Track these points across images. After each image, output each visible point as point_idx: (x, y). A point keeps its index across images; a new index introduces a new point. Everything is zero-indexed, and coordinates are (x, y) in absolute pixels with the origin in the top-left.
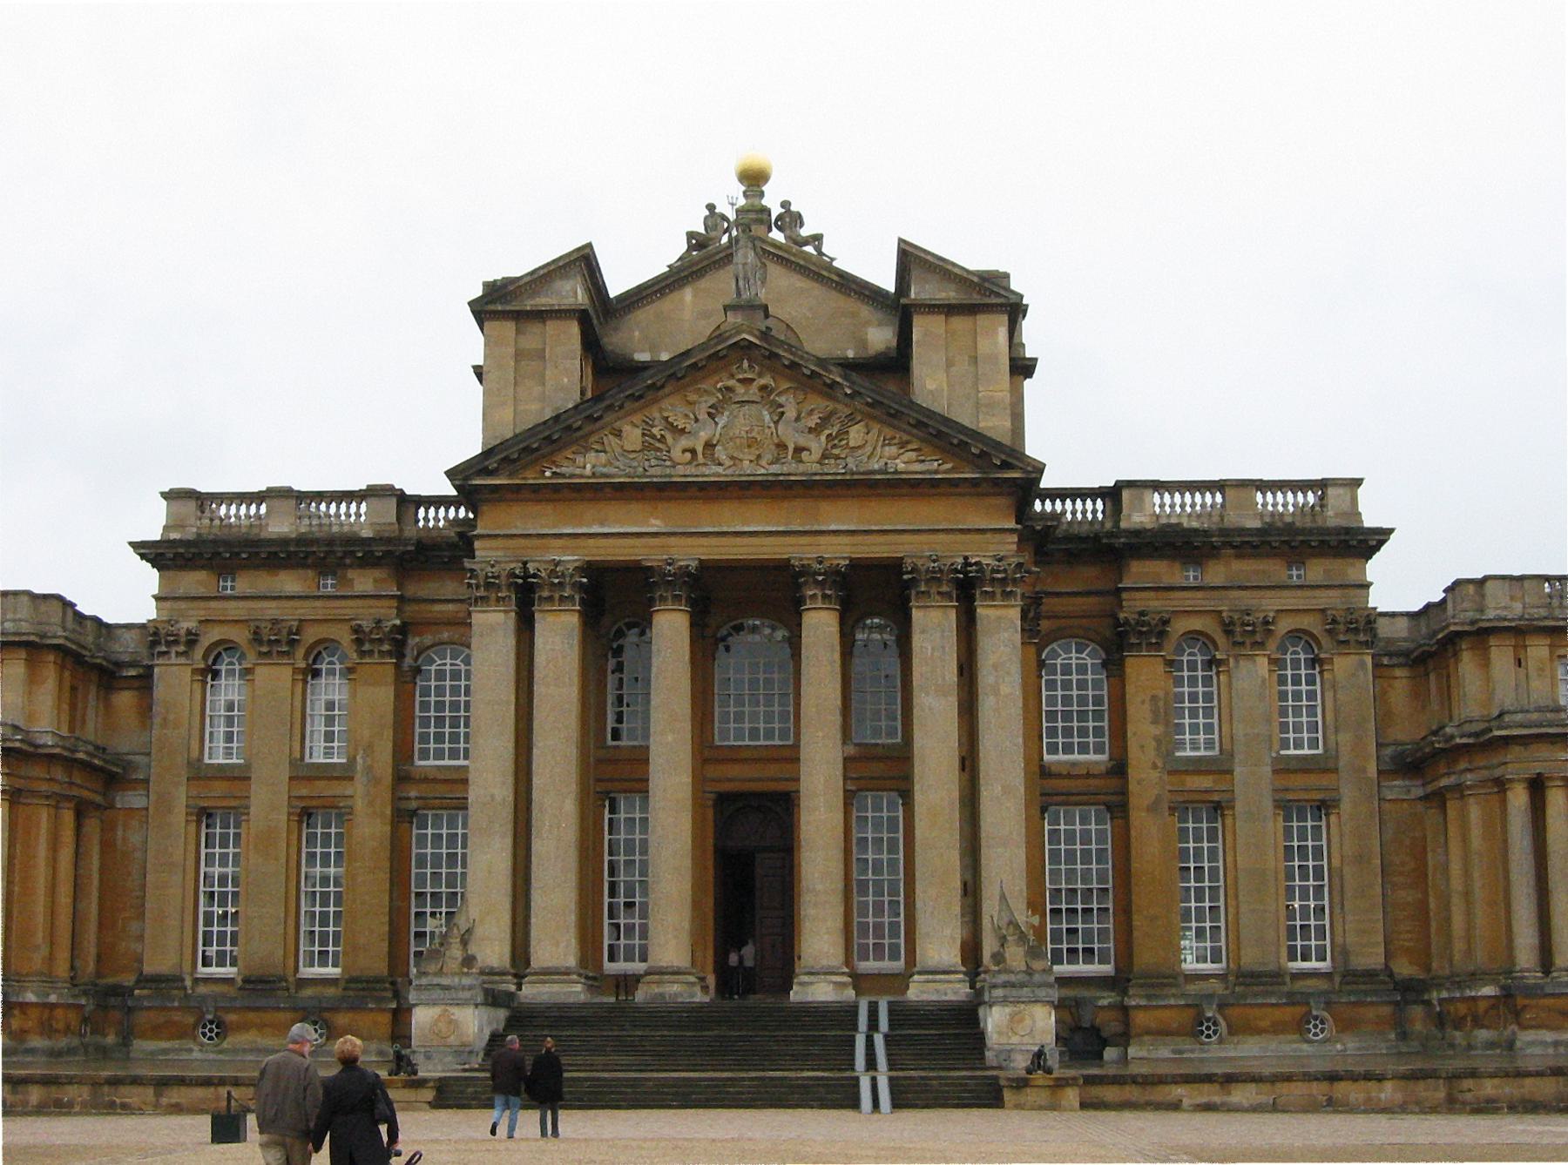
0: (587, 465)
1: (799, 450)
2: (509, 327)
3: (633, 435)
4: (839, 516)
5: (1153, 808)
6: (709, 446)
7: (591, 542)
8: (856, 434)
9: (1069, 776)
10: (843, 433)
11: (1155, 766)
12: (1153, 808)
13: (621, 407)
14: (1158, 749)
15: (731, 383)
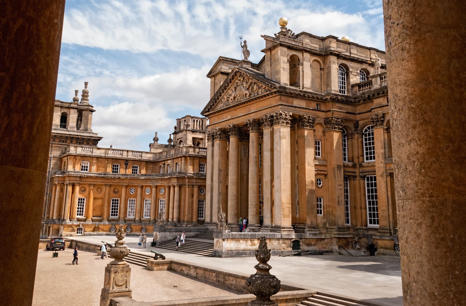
0: (220, 106)
1: (246, 94)
2: (213, 78)
3: (225, 97)
4: (254, 107)
5: (382, 176)
6: (234, 98)
7: (222, 123)
8: (255, 87)
9: (368, 167)
10: (253, 88)
11: (382, 162)
12: (382, 176)
13: (223, 92)
14: (382, 157)
15: (237, 81)
